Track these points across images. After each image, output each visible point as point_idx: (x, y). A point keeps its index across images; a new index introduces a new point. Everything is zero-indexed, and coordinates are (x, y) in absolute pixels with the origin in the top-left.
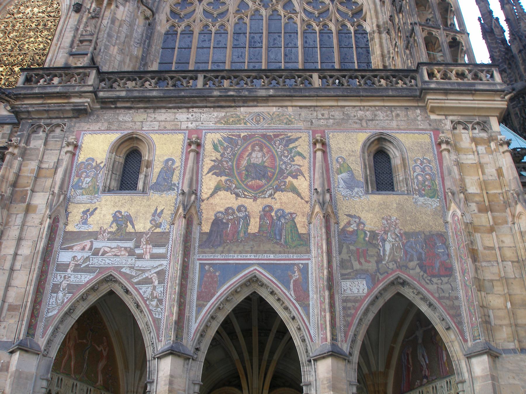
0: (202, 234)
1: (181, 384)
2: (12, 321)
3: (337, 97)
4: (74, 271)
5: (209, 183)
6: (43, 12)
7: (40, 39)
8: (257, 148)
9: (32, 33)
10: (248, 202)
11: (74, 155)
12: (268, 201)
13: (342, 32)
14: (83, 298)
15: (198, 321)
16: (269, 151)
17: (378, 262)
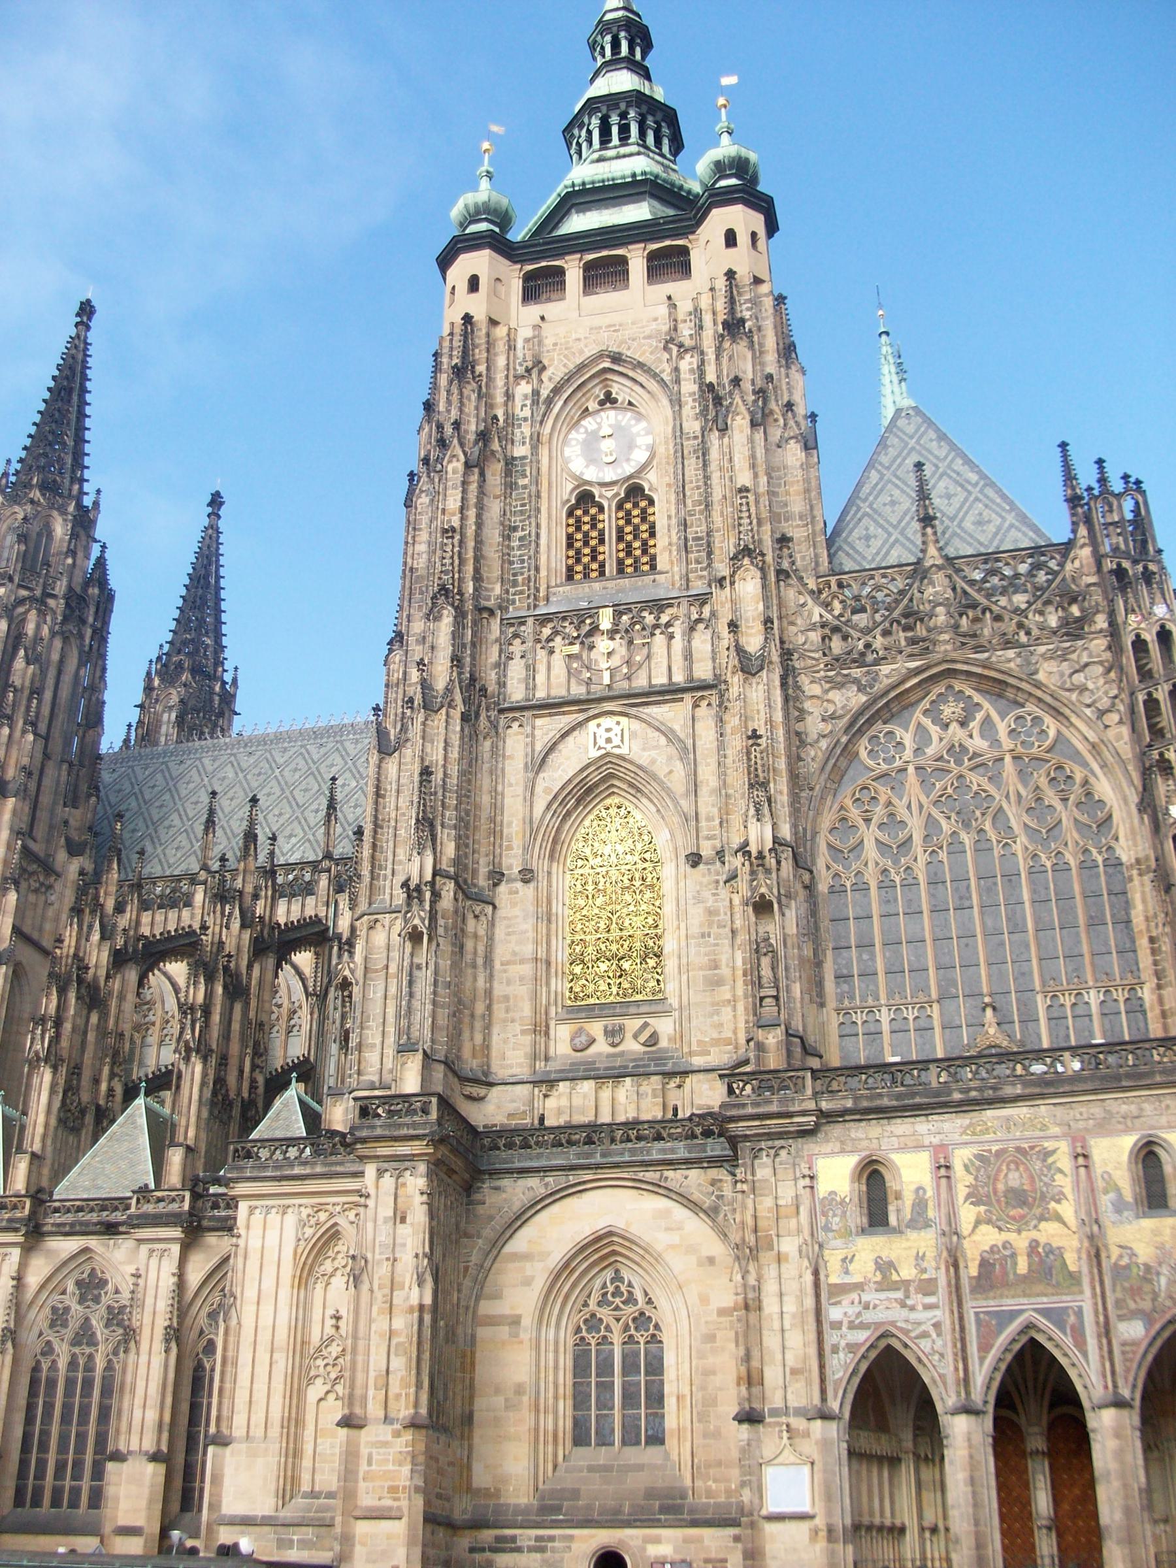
0: (970, 1278)
1: (978, 1438)
2: (798, 1385)
3: (1094, 1091)
4: (850, 1328)
5: (967, 1214)
6: (632, 852)
7: (644, 907)
8: (1012, 1166)
9: (628, 897)
10: (1012, 1237)
11: (812, 1188)
12: (1034, 1234)
13: (1087, 866)
14: (863, 1357)
15: (984, 1371)
16: (1027, 1169)
17: (1154, 1300)
